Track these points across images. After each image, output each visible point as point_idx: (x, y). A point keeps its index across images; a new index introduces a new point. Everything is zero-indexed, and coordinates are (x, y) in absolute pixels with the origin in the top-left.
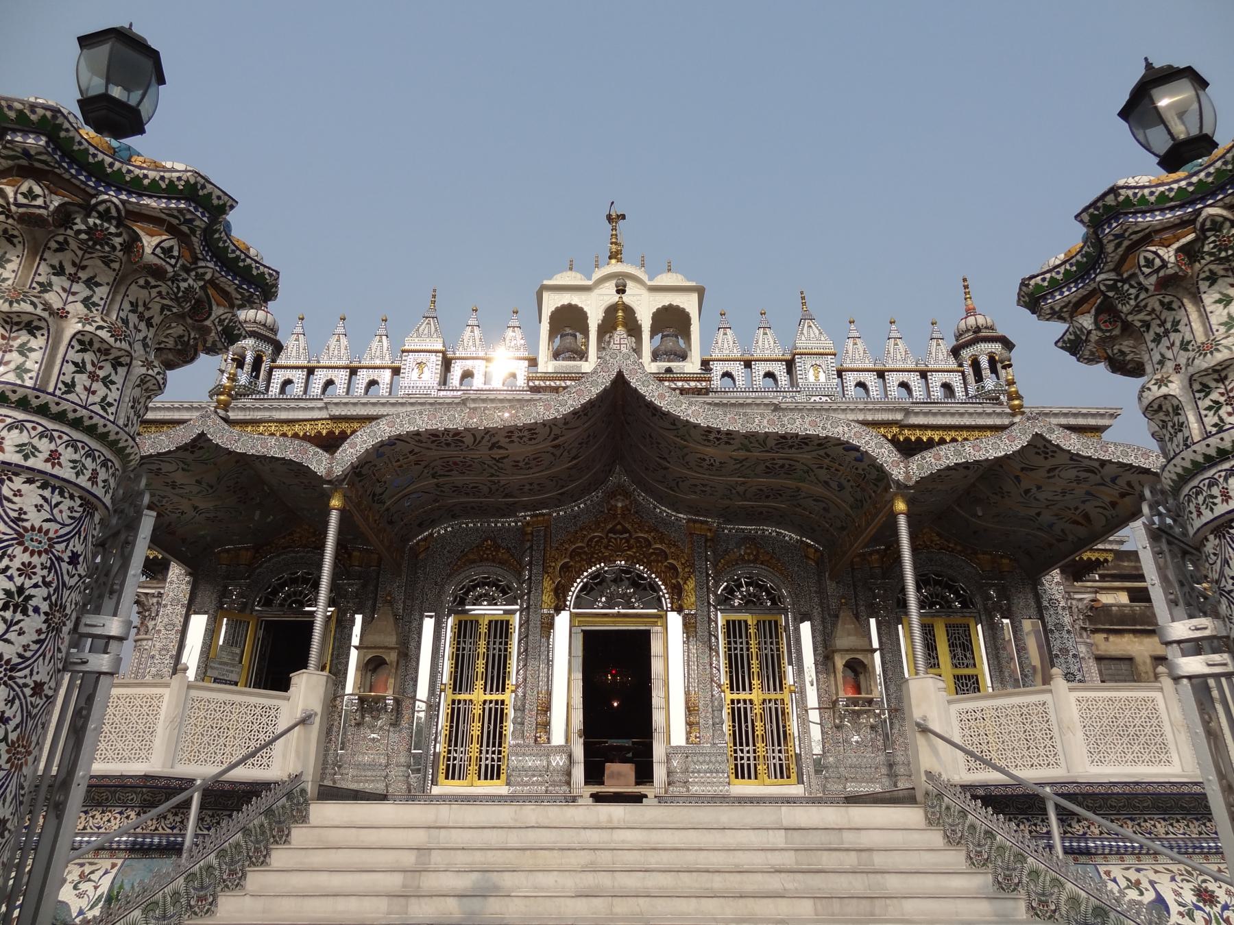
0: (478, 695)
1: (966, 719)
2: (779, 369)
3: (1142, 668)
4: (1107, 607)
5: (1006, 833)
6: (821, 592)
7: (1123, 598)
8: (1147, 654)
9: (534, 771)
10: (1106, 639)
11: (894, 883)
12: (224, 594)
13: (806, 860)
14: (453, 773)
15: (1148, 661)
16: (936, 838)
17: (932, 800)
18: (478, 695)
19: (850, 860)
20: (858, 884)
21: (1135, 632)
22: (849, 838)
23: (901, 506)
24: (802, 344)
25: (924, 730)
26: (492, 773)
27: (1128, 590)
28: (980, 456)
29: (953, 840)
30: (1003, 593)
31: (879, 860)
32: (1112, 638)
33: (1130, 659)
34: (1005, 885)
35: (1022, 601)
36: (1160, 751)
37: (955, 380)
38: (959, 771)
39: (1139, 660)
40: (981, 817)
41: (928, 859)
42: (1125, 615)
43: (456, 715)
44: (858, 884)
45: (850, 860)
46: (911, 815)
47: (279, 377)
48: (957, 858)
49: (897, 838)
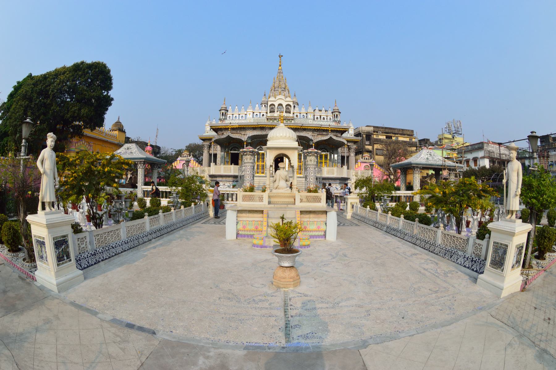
0: (260, 163)
2: (305, 115)
7: (385, 137)
12: (225, 149)
14: (258, 173)
18: (260, 163)
24: (309, 111)
26: (263, 173)
30: (333, 151)
35: (335, 152)
36: (333, 174)
37: (332, 118)
43: (258, 166)
47: (228, 116)
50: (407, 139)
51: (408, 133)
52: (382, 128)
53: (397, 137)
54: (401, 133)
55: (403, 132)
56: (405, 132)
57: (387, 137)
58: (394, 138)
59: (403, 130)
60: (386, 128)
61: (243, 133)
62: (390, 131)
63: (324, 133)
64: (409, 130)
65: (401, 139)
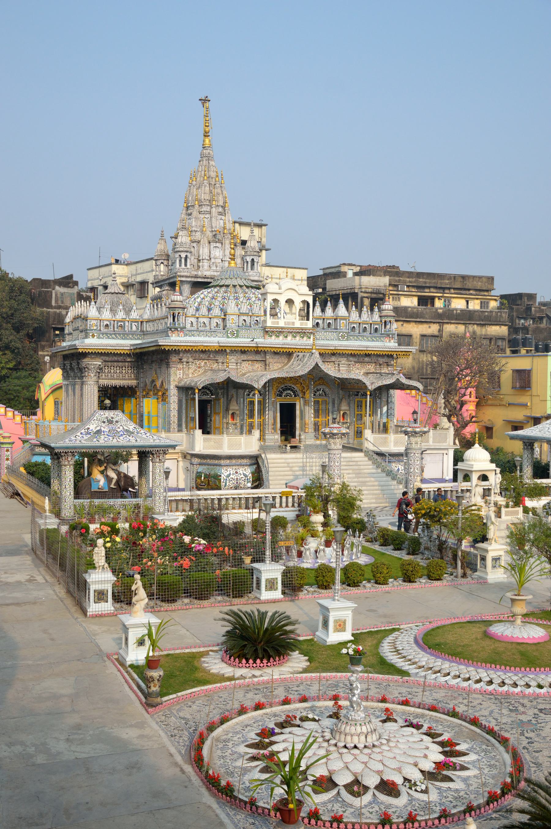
1: (374, 438)
3: (415, 340)
4: (406, 308)
5: (379, 459)
6: (338, 393)
7: (415, 301)
8: (418, 333)
9: (272, 439)
10: (402, 325)
11: (362, 467)
13: (348, 463)
15: (418, 337)
16: (366, 459)
17: (367, 453)
19: (354, 463)
20: (357, 467)
21: (416, 322)
22: (353, 459)
23: (368, 393)
25: (367, 440)
27: (418, 296)
28: (386, 383)
29: (370, 459)
31: (359, 463)
32: (405, 325)
33: (411, 336)
34: (378, 467)
38: (372, 448)
39: (414, 336)
40: (376, 457)
41: (366, 463)
42: (414, 313)
44: (357, 467)
45: (354, 463)
46: (361, 454)
48: (370, 462)
49: (361, 459)
50: (475, 305)
51: (479, 285)
52: (410, 274)
53: (448, 301)
54: (458, 285)
55: (463, 285)
56: (469, 285)
57: (423, 301)
58: (439, 304)
59: (464, 277)
60: (419, 275)
61: (220, 359)
62: (428, 282)
63: (367, 359)
64: (480, 277)
65: (458, 304)
